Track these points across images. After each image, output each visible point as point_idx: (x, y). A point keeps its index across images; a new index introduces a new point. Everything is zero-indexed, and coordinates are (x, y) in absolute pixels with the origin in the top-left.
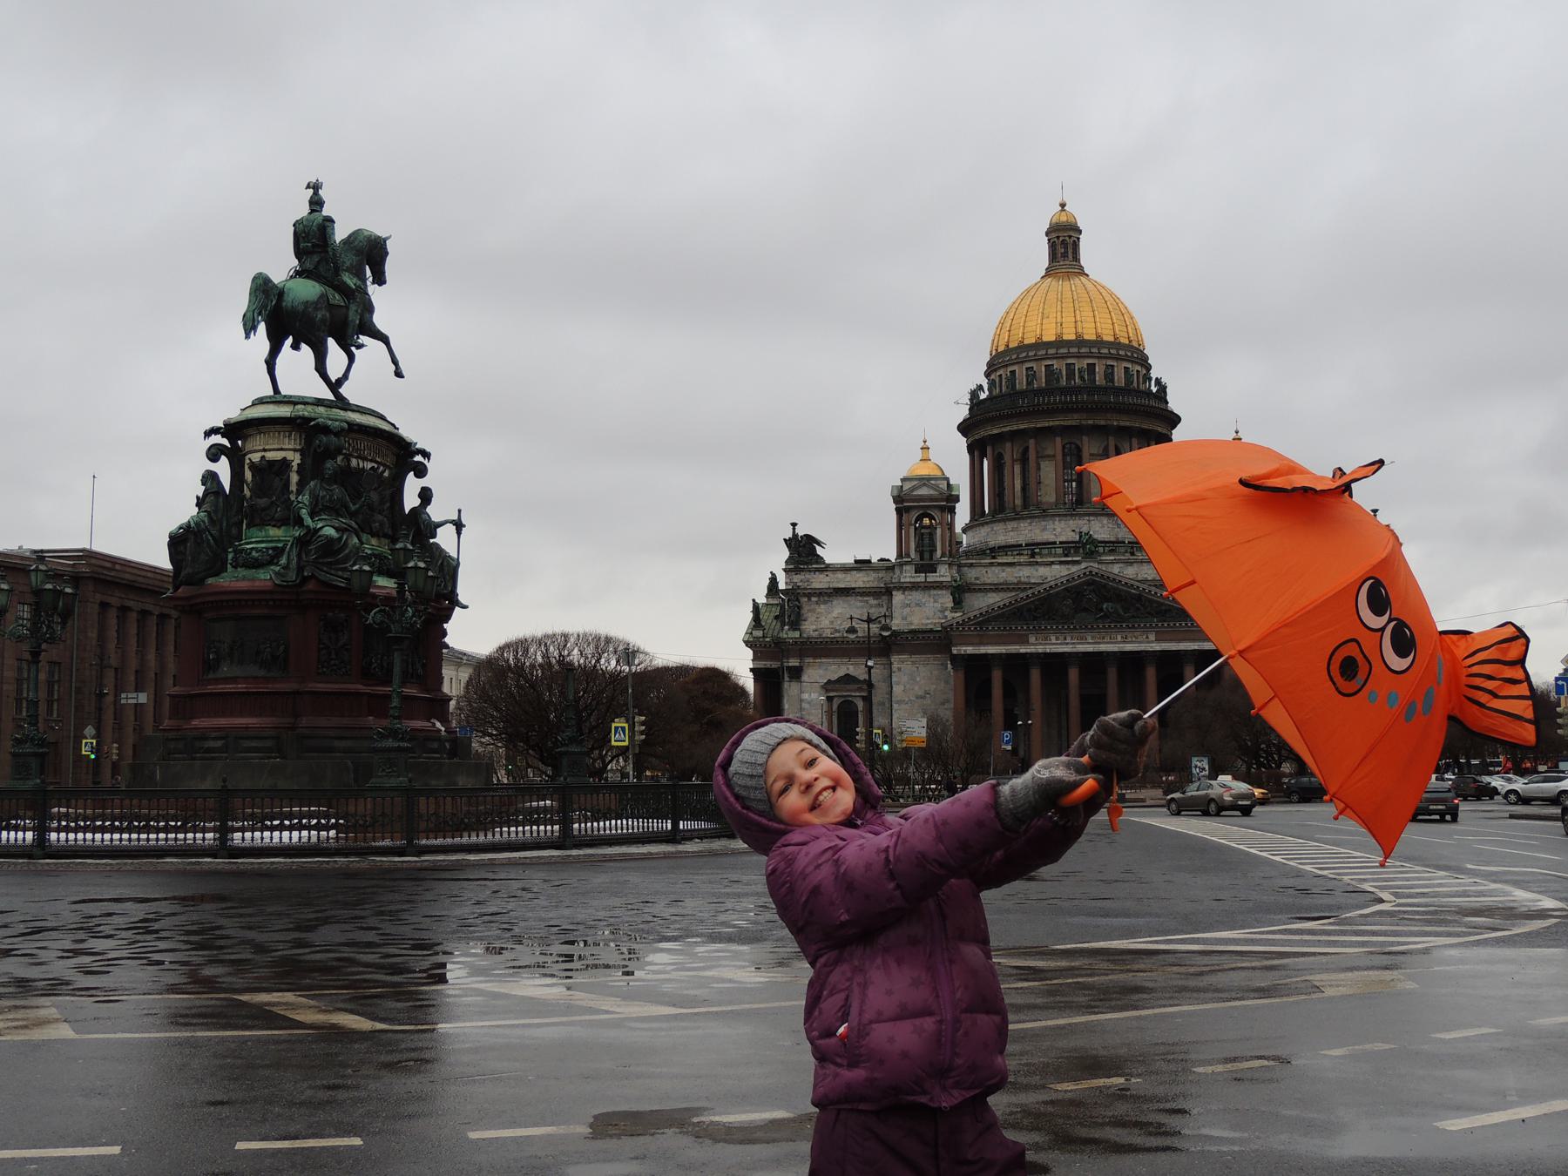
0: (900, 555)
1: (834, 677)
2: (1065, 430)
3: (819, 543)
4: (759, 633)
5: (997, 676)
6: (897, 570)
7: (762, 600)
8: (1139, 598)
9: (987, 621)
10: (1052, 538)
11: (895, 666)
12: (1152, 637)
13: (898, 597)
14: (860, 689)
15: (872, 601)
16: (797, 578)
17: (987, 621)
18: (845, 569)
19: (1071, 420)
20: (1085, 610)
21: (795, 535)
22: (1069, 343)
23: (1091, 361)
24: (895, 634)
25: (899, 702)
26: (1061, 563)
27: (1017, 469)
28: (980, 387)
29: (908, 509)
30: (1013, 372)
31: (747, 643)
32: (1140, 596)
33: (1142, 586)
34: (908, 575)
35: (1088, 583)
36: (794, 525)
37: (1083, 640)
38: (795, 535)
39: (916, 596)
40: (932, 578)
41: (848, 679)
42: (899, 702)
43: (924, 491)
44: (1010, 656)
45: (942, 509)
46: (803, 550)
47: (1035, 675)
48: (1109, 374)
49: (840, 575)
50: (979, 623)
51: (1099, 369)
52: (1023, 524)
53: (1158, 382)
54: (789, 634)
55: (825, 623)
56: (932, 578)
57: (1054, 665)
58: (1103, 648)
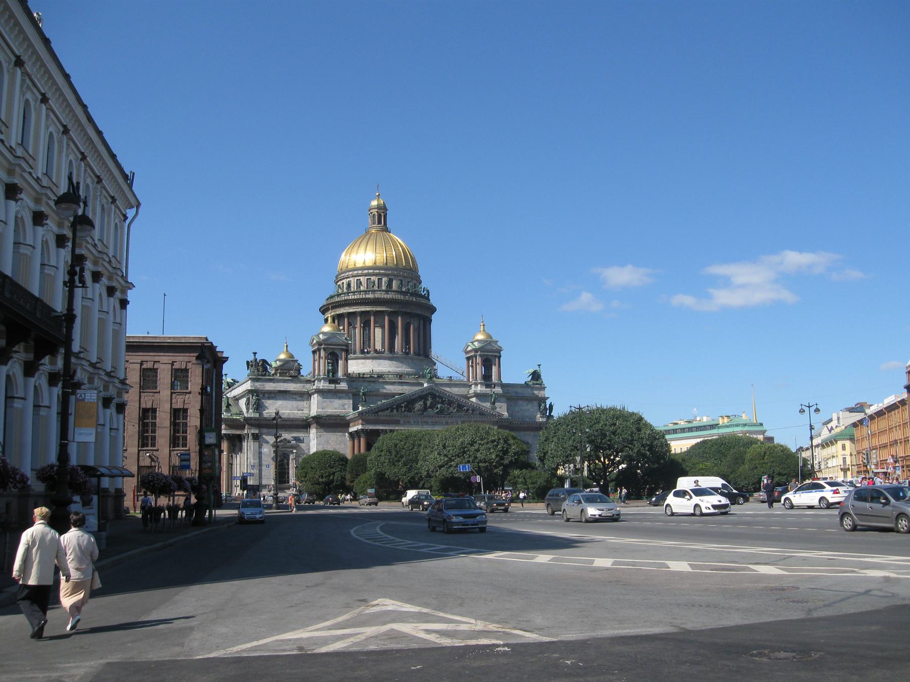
2: (390, 314)
17: (382, 410)
20: (430, 407)
22: (391, 269)
36: (255, 353)
43: (334, 341)
54: (251, 414)
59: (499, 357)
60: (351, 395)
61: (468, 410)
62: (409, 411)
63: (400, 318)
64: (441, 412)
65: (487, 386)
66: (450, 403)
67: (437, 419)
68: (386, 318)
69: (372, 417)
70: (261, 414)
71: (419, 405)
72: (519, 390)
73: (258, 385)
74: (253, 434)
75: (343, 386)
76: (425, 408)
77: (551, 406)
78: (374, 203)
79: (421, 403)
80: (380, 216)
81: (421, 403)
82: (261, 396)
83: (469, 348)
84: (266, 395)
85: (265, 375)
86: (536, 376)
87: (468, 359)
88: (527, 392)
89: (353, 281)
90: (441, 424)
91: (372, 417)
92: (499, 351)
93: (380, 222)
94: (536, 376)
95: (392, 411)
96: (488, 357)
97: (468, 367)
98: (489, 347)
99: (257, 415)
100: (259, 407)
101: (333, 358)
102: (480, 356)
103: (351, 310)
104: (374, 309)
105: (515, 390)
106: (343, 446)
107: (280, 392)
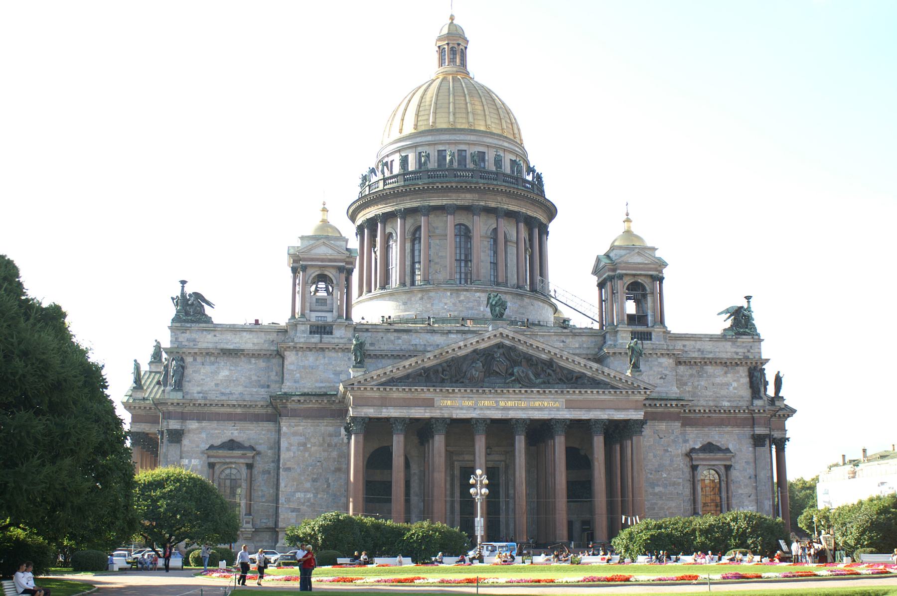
0: (293, 316)
1: (218, 442)
4: (140, 395)
5: (398, 443)
7: (145, 367)
8: (550, 364)
9: (392, 382)
11: (284, 429)
13: (291, 358)
14: (243, 456)
15: (262, 364)
16: (183, 337)
18: (234, 329)
19: (466, 199)
23: (481, 149)
24: (287, 396)
26: (458, 332)
28: (373, 171)
29: (304, 268)
30: (407, 157)
32: (551, 359)
33: (553, 351)
34: (302, 336)
35: (499, 346)
39: (311, 358)
41: (231, 445)
42: (288, 469)
43: (322, 251)
45: (340, 269)
46: (191, 309)
47: (439, 442)
48: (498, 162)
49: (229, 336)
50: (382, 384)
51: (490, 156)
53: (539, 177)
55: (210, 385)
56: (326, 338)
57: (460, 429)
58: (512, 415)
59: (661, 280)
61: (577, 378)
65: (634, 335)
72: (708, 346)
74: (170, 432)
77: (778, 381)
80: (453, 51)
82: (189, 360)
83: (602, 264)
84: (199, 359)
85: (198, 321)
86: (741, 320)
87: (601, 286)
88: (727, 350)
89: (397, 158)
94: (741, 320)
97: (601, 301)
98: (638, 259)
105: (699, 345)
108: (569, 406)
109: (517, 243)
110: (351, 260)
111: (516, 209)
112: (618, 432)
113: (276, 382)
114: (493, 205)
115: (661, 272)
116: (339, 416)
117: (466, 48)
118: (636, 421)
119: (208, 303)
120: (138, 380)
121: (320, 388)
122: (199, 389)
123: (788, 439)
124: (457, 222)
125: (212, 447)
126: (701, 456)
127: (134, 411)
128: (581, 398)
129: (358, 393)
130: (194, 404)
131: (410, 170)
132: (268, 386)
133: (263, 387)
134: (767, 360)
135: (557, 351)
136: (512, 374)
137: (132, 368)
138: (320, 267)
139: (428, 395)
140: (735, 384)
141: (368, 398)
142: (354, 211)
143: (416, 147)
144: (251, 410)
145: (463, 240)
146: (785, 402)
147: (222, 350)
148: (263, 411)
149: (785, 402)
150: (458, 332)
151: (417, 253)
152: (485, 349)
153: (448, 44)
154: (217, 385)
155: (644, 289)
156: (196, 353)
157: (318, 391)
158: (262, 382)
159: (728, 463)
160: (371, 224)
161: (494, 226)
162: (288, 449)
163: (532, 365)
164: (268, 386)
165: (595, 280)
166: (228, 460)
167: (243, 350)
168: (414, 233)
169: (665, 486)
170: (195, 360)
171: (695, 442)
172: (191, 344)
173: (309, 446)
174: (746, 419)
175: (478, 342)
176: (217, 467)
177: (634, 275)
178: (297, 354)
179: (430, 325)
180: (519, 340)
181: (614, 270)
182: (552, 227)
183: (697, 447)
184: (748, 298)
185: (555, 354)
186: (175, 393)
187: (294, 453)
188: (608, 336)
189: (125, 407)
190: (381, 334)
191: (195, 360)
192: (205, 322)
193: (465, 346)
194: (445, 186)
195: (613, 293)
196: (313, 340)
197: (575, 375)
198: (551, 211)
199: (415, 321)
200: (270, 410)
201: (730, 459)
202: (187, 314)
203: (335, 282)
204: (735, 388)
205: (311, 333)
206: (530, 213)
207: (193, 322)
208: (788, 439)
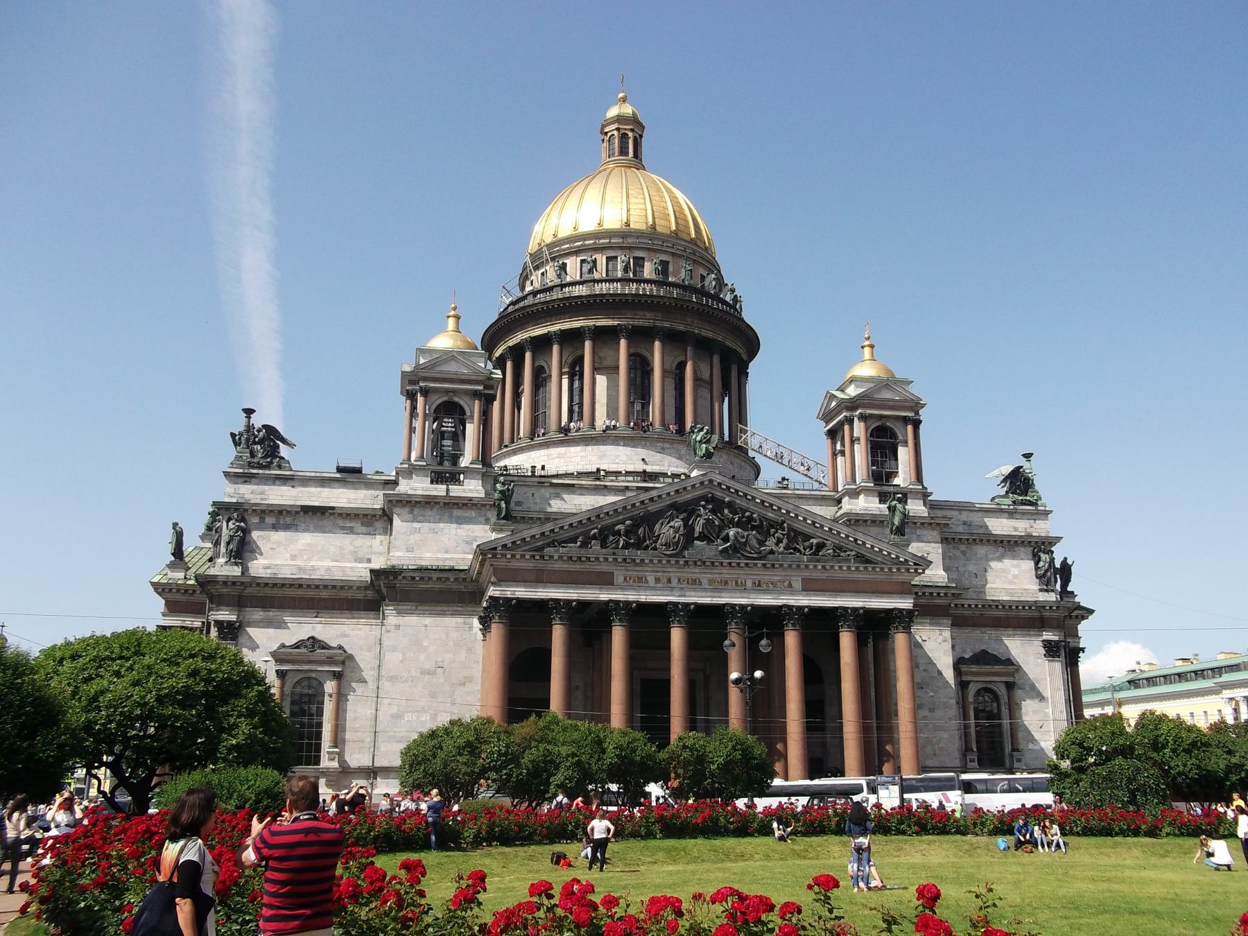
3: (284, 441)
4: (179, 575)
6: (402, 481)
10: (613, 468)
12: (797, 584)
14: (330, 661)
17: (551, 544)
19: (643, 320)
20: (702, 537)
21: (249, 428)
23: (664, 257)
25: (392, 679)
27: (565, 382)
31: (160, 588)
37: (695, 583)
38: (249, 428)
40: (456, 491)
41: (314, 643)
42: (392, 679)
43: (452, 368)
44: (583, 605)
45: (476, 394)
46: (261, 449)
47: (618, 636)
52: (574, 450)
54: (223, 569)
56: (456, 491)
57: (649, 623)
59: (917, 424)
60: (492, 515)
61: (821, 546)
62: (639, 545)
63: (657, 344)
64: (737, 549)
66: (765, 528)
67: (727, 573)
68: (623, 343)
69: (525, 563)
70: (245, 571)
71: (668, 530)
73: (250, 493)
75: (472, 488)
76: (689, 537)
78: (613, 112)
79: (678, 523)
80: (624, 137)
81: (678, 523)
85: (268, 467)
87: (833, 434)
90: (740, 587)
91: (525, 563)
92: (916, 406)
93: (624, 151)
95: (585, 545)
96: (885, 426)
97: (834, 455)
98: (886, 395)
99: (236, 571)
100: (241, 550)
101: (450, 410)
102: (863, 418)
103: (539, 331)
104: (590, 323)
105: (964, 516)
106: (463, 655)
107: (307, 510)
108: (810, 587)
109: (711, 384)
110: (491, 382)
111: (710, 335)
112: (874, 629)
113: (381, 554)
114: (681, 328)
115: (917, 413)
116: (470, 602)
117: (641, 136)
118: (901, 610)
119: (284, 441)
120: (178, 552)
121: (446, 559)
122: (266, 562)
123: (1083, 650)
124: (632, 351)
125: (283, 646)
126: (974, 668)
127: (169, 596)
128: (824, 575)
129: (501, 563)
130: (258, 585)
131: (568, 279)
132: (369, 561)
133: (360, 561)
134: (1059, 539)
135: (791, 508)
136: (726, 539)
137: (169, 536)
138: (447, 391)
139: (604, 568)
140: (1015, 571)
141: (517, 570)
142: (490, 340)
143: (576, 252)
144: (343, 594)
145: (639, 375)
146: (1077, 600)
147: (302, 507)
148: (360, 596)
149: (1077, 600)
150: (638, 488)
151: (576, 393)
152: (687, 503)
153: (618, 129)
154: (293, 557)
155: (893, 435)
156: (263, 511)
157: (441, 564)
158: (360, 555)
159: (1010, 679)
160: (517, 353)
161: (682, 358)
162: (394, 649)
163: (753, 528)
164: (369, 561)
165: (823, 428)
166: (306, 667)
167: (333, 508)
168: (572, 367)
169: (932, 710)
170: (262, 520)
171: (964, 651)
172: (256, 499)
173: (425, 644)
174: (1032, 619)
175: (677, 491)
176: (289, 675)
177: (881, 417)
178: (411, 512)
179: (596, 480)
180: (737, 491)
181: (854, 409)
182: (753, 368)
183: (967, 656)
184: (1028, 456)
185: (788, 512)
186: (227, 567)
187: (404, 654)
188: (845, 500)
189: (156, 590)
190: (533, 490)
191: (262, 520)
192: (280, 467)
193: (660, 496)
194: (617, 299)
195: (852, 441)
196: (435, 493)
197: (814, 541)
198: (752, 344)
199: (581, 475)
200: (370, 594)
201: (1013, 675)
202: (253, 455)
203: (468, 413)
204: (1015, 577)
205: (432, 482)
206: (728, 343)
207: (261, 467)
208: (1083, 650)
